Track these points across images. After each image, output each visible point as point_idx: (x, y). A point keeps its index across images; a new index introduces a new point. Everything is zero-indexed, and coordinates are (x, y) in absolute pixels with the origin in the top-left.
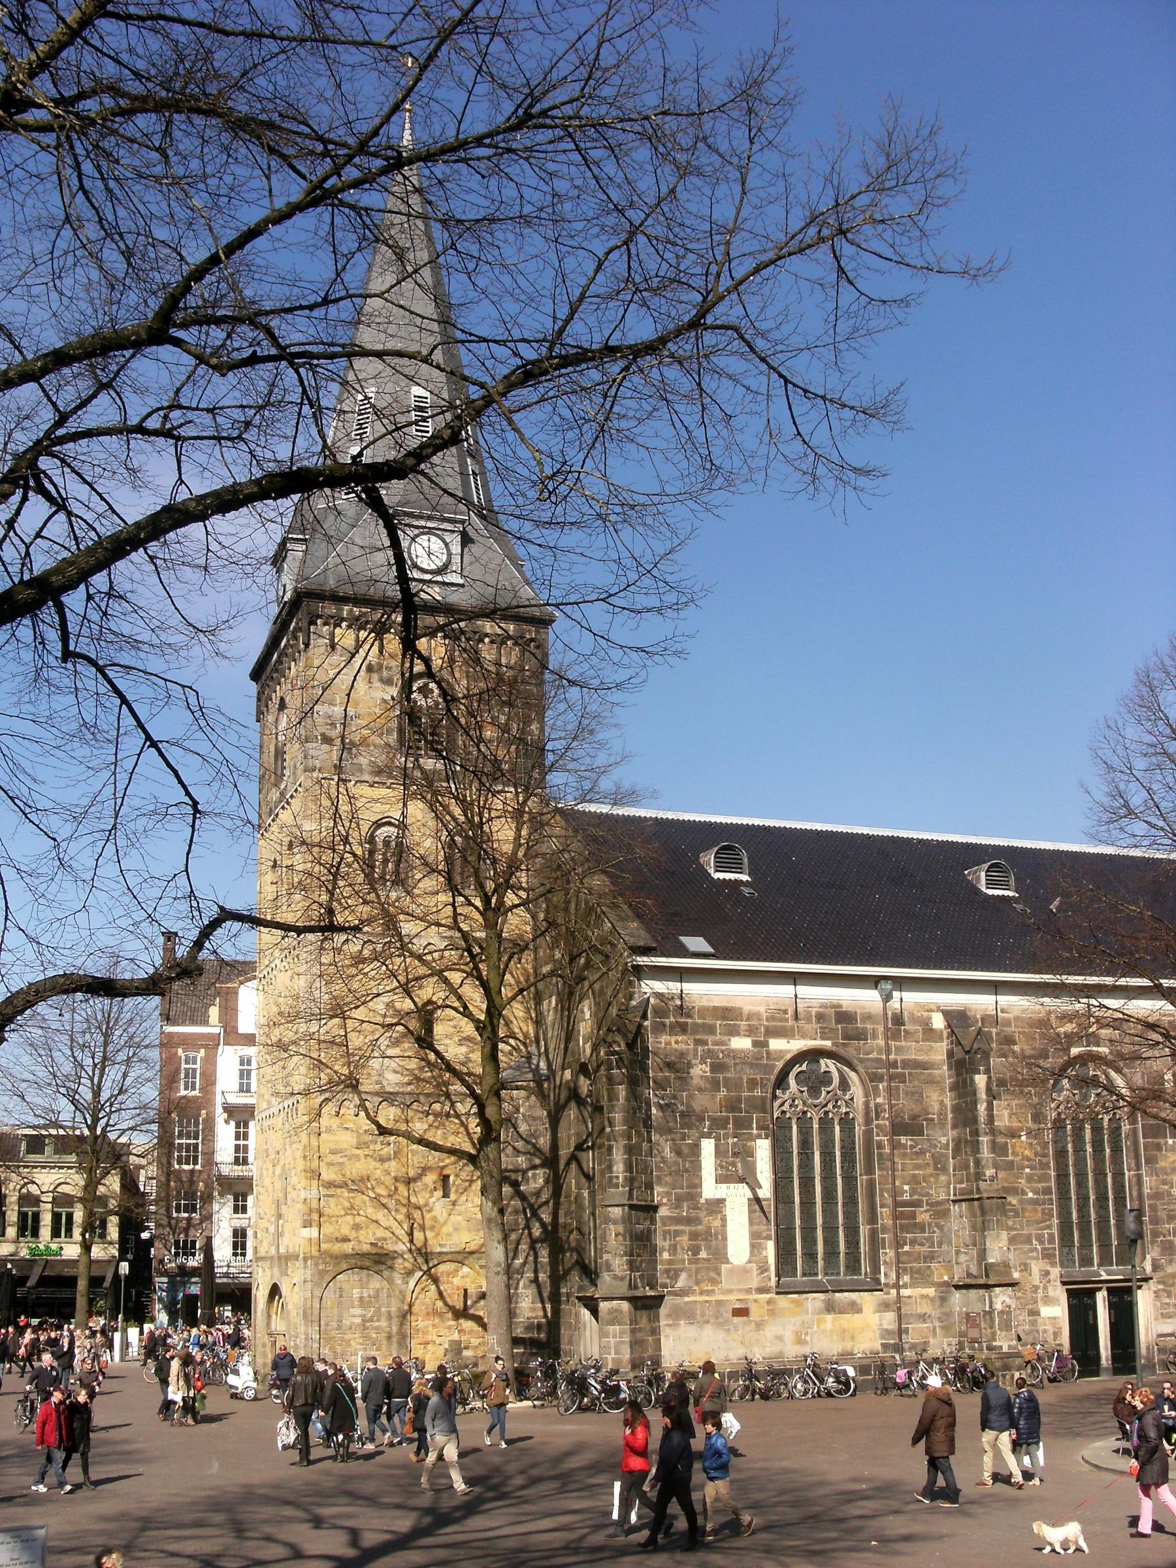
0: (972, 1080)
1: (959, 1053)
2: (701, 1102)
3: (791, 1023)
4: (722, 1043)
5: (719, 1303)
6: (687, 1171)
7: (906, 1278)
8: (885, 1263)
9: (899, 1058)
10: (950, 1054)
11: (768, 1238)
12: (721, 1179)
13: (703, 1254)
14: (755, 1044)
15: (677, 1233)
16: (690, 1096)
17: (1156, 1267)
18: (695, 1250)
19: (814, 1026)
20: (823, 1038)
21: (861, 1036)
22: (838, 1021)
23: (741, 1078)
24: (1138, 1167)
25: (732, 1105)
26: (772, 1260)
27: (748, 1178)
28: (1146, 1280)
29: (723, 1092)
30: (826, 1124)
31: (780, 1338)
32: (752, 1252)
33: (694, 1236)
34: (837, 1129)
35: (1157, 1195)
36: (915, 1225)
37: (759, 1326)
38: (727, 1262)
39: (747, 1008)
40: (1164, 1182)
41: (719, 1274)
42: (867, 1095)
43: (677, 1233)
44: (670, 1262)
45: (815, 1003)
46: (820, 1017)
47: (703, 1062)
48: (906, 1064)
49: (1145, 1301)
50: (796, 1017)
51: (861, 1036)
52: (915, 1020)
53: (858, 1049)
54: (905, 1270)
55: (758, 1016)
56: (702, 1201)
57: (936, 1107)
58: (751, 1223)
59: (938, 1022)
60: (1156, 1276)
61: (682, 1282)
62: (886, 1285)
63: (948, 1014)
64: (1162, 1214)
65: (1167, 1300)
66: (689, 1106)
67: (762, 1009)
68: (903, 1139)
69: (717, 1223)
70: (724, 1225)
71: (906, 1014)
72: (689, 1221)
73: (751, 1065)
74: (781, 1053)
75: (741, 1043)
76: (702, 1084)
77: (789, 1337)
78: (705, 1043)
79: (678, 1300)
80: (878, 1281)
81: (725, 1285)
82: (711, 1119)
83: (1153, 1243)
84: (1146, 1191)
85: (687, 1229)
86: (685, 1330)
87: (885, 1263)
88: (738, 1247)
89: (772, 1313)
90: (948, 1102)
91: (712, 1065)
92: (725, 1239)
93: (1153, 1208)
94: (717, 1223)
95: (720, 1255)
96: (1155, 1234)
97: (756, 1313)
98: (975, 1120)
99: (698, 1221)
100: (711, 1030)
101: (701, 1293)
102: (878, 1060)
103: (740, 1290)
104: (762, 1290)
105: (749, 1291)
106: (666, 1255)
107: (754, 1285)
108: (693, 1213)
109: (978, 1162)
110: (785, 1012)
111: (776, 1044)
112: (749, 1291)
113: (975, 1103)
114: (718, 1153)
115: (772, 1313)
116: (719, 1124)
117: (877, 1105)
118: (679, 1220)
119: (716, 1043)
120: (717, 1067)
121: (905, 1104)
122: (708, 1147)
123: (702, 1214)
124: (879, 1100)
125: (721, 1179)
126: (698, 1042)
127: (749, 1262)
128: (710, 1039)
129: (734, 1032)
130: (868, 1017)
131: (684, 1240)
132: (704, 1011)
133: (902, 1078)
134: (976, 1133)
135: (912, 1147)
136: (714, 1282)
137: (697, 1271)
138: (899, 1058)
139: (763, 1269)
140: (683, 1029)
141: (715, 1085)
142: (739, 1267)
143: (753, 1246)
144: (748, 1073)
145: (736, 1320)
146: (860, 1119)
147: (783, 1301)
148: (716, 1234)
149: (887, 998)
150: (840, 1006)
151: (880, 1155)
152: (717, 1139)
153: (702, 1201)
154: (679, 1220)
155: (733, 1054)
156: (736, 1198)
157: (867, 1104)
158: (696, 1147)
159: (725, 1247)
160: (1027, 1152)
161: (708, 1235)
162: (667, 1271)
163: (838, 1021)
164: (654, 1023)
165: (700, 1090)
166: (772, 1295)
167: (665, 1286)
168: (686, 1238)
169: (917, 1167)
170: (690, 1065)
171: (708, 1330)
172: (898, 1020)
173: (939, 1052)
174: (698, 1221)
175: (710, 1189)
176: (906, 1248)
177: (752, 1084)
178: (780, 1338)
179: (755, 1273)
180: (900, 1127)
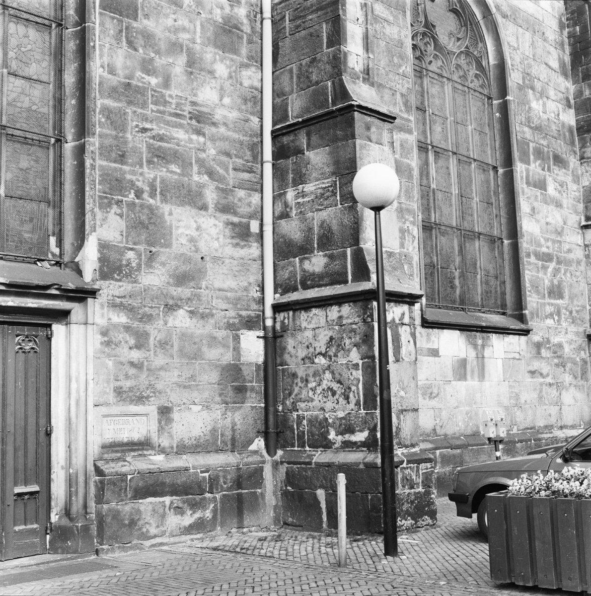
17: (110, 268)
28: (82, 295)
35: (129, 91)
40: (147, 67)
60: (109, 289)
64: (136, 141)
65: (136, 355)
93: (116, 121)
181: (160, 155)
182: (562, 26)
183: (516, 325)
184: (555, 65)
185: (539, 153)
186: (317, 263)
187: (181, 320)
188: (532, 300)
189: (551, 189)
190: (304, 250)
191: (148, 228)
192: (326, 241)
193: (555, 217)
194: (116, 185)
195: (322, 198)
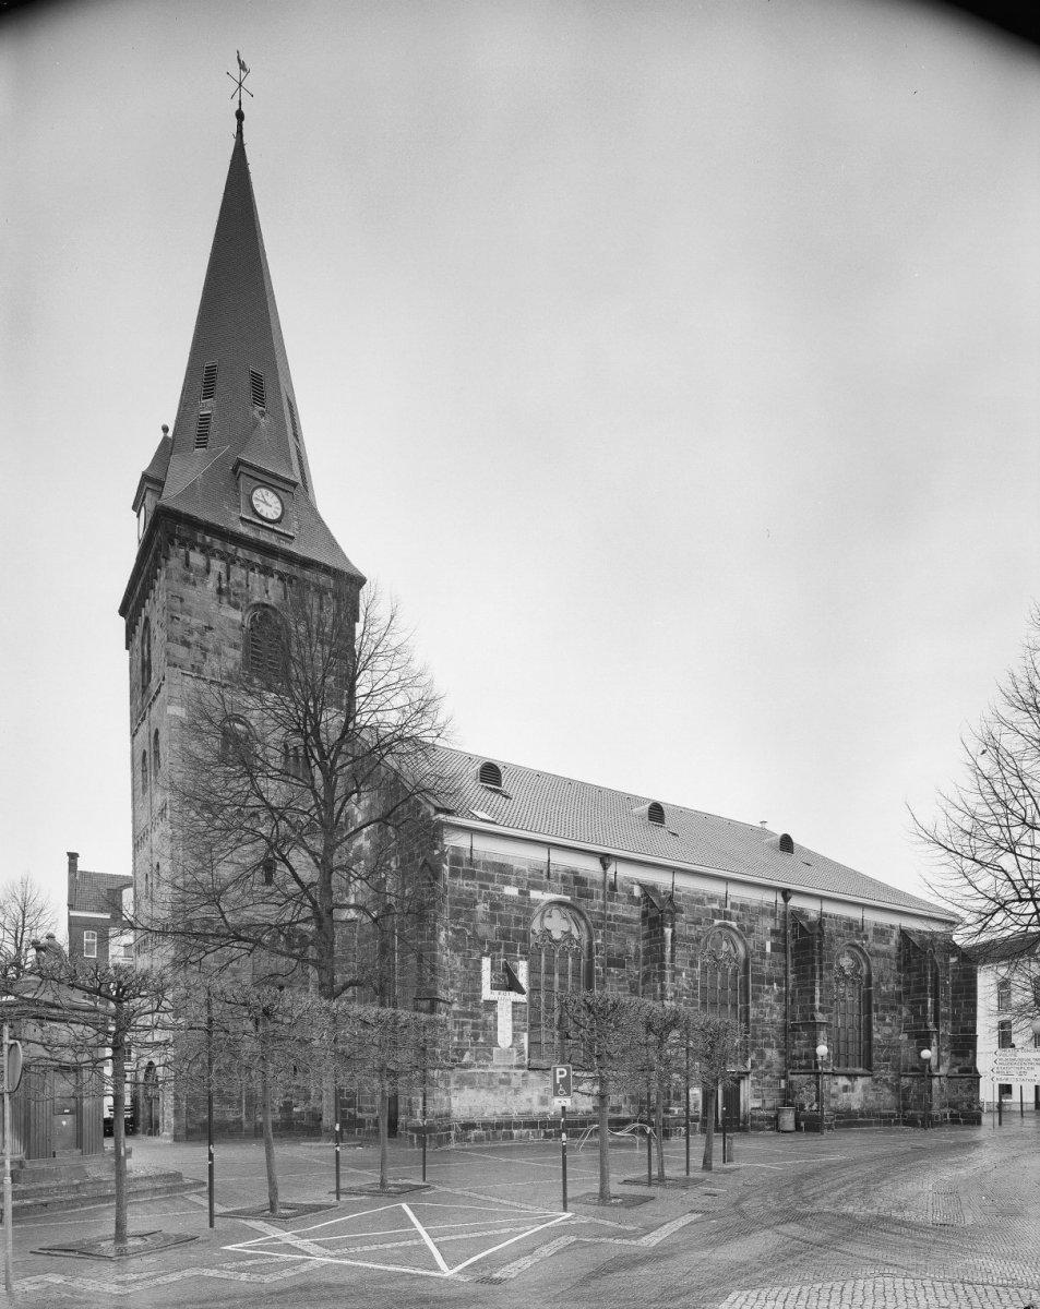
0: (663, 931)
1: (653, 913)
2: (483, 930)
3: (545, 880)
4: (499, 889)
5: (491, 1074)
9: (613, 914)
10: (645, 914)
11: (525, 1030)
12: (494, 987)
13: (481, 1040)
14: (521, 892)
15: (464, 1024)
16: (476, 926)
17: (753, 1066)
18: (476, 1036)
19: (558, 885)
20: (565, 894)
21: (589, 895)
22: (575, 884)
24: (747, 1002)
25: (504, 935)
26: (526, 1046)
27: (512, 985)
28: (747, 1073)
29: (498, 925)
30: (564, 955)
31: (529, 1100)
33: (475, 1026)
34: (570, 959)
35: (757, 1021)
37: (517, 1091)
38: (497, 1045)
39: (516, 866)
40: (761, 1012)
42: (590, 937)
43: (464, 1024)
44: (459, 1043)
45: (561, 868)
46: (564, 879)
47: (485, 901)
48: (617, 918)
49: (746, 1088)
50: (548, 877)
51: (589, 895)
52: (623, 889)
53: (587, 904)
55: (523, 871)
57: (633, 950)
58: (513, 1019)
59: (637, 892)
61: (467, 1058)
63: (643, 887)
64: (759, 1033)
66: (475, 933)
67: (526, 868)
68: (612, 970)
69: (491, 1018)
70: (496, 1020)
71: (618, 884)
72: (472, 1015)
73: (517, 907)
74: (537, 902)
75: (511, 891)
76: (484, 917)
77: (536, 1100)
78: (486, 887)
79: (463, 1072)
81: (495, 1062)
82: (490, 944)
83: (753, 1050)
84: (751, 1017)
85: (471, 1021)
86: (468, 1093)
88: (504, 1035)
89: (525, 1083)
90: (641, 947)
91: (491, 904)
92: (496, 1029)
93: (754, 1028)
95: (492, 1041)
96: (754, 1045)
97: (516, 1081)
98: (663, 958)
99: (477, 1016)
100: (491, 879)
101: (479, 1067)
102: (600, 914)
103: (504, 1066)
104: (519, 1067)
105: (511, 1067)
106: (456, 1039)
107: (514, 1063)
108: (475, 1010)
109: (663, 987)
110: (542, 872)
111: (535, 894)
112: (511, 1067)
113: (663, 948)
114: (493, 968)
115: (525, 1083)
116: (495, 947)
117: (597, 944)
118: (465, 1014)
119: (494, 889)
120: (494, 906)
121: (614, 945)
122: (486, 963)
123: (481, 1011)
124: (599, 941)
125: (494, 987)
126: (482, 887)
128: (491, 885)
129: (507, 882)
130: (594, 883)
131: (468, 1028)
132: (487, 865)
133: (613, 928)
134: (663, 967)
135: (618, 975)
136: (488, 1059)
137: (477, 1051)
138: (613, 914)
139: (521, 1053)
140: (471, 875)
141: (493, 919)
143: (514, 1036)
144: (515, 913)
145: (502, 1087)
146: (585, 954)
147: (532, 1076)
149: (605, 868)
150: (577, 873)
151: (598, 979)
152: (493, 958)
154: (465, 1014)
155: (507, 898)
156: (505, 1000)
157: (590, 944)
158: (479, 962)
160: (685, 986)
161: (485, 1026)
162: (457, 1050)
163: (575, 884)
164: (451, 869)
165: (483, 921)
166: (525, 1071)
167: (454, 1061)
168: (469, 1027)
169: (620, 989)
170: (476, 903)
171: (483, 1092)
172: (613, 887)
173: (635, 913)
174: (477, 1016)
175: (487, 993)
177: (518, 921)
178: (529, 1100)
179: (515, 1054)
180: (611, 963)
181: (763, 1036)
182: (900, 950)
183: (866, 1072)
184: (894, 967)
185: (884, 1008)
186: (804, 1062)
187: (768, 1078)
188: (875, 1063)
189: (887, 1020)
190: (800, 1058)
191: (761, 1055)
192: (806, 1057)
193: (888, 1030)
194: (754, 1045)
195: (807, 1045)
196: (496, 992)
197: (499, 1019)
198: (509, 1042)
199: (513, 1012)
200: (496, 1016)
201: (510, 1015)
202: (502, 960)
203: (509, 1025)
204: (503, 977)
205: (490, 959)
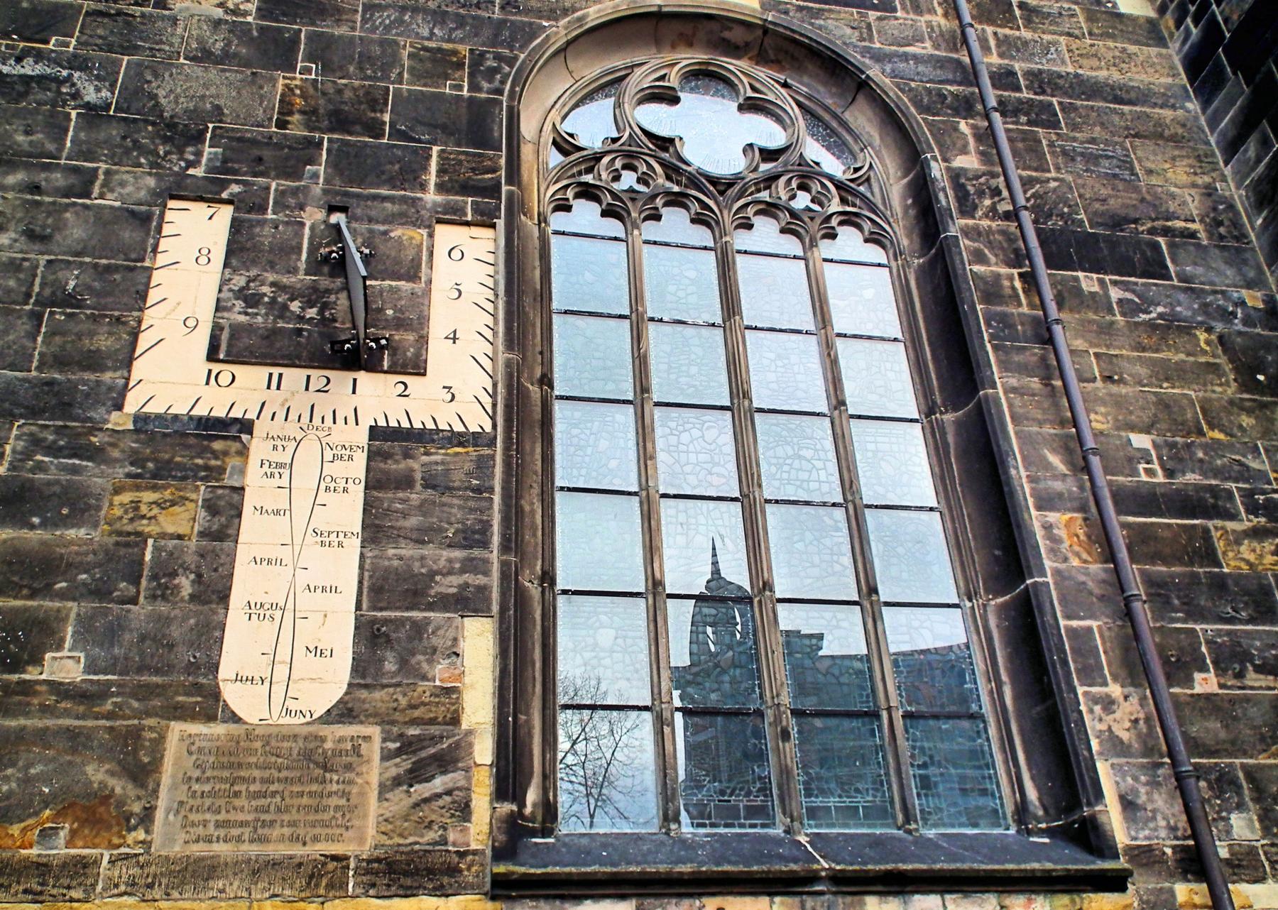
6: (70, 300)
7: (1243, 827)
8: (1116, 746)
11: (467, 603)
12: (227, 348)
23: (390, 47)
26: (479, 710)
29: (304, 73)
32: (364, 669)
36: (1220, 585)
41: (142, 773)
42: (913, 159)
54: (1224, 782)
56: (120, 421)
58: (375, 528)
62: (1145, 856)
80: (1089, 836)
81: (167, 837)
87: (1116, 746)
92: (215, 592)
94: (182, 520)
107: (364, 838)
117: (956, 177)
124: (969, 161)
125: (227, 348)
127: (343, 712)
136: (95, 814)
142: (271, 740)
143: (371, 637)
148: (166, 571)
152: (249, 206)
153: (120, 421)
157: (921, 190)
158: (146, 222)
159: (210, 637)
175: (171, 372)
176: (1206, 683)
179: (374, 771)
180: (1068, 249)
196: (252, 377)
197: (255, 533)
198: (328, 681)
199: (375, 483)
200: (226, 513)
201: (347, 511)
202: (313, 216)
203: (342, 568)
204: (313, 296)
205: (226, 214)
